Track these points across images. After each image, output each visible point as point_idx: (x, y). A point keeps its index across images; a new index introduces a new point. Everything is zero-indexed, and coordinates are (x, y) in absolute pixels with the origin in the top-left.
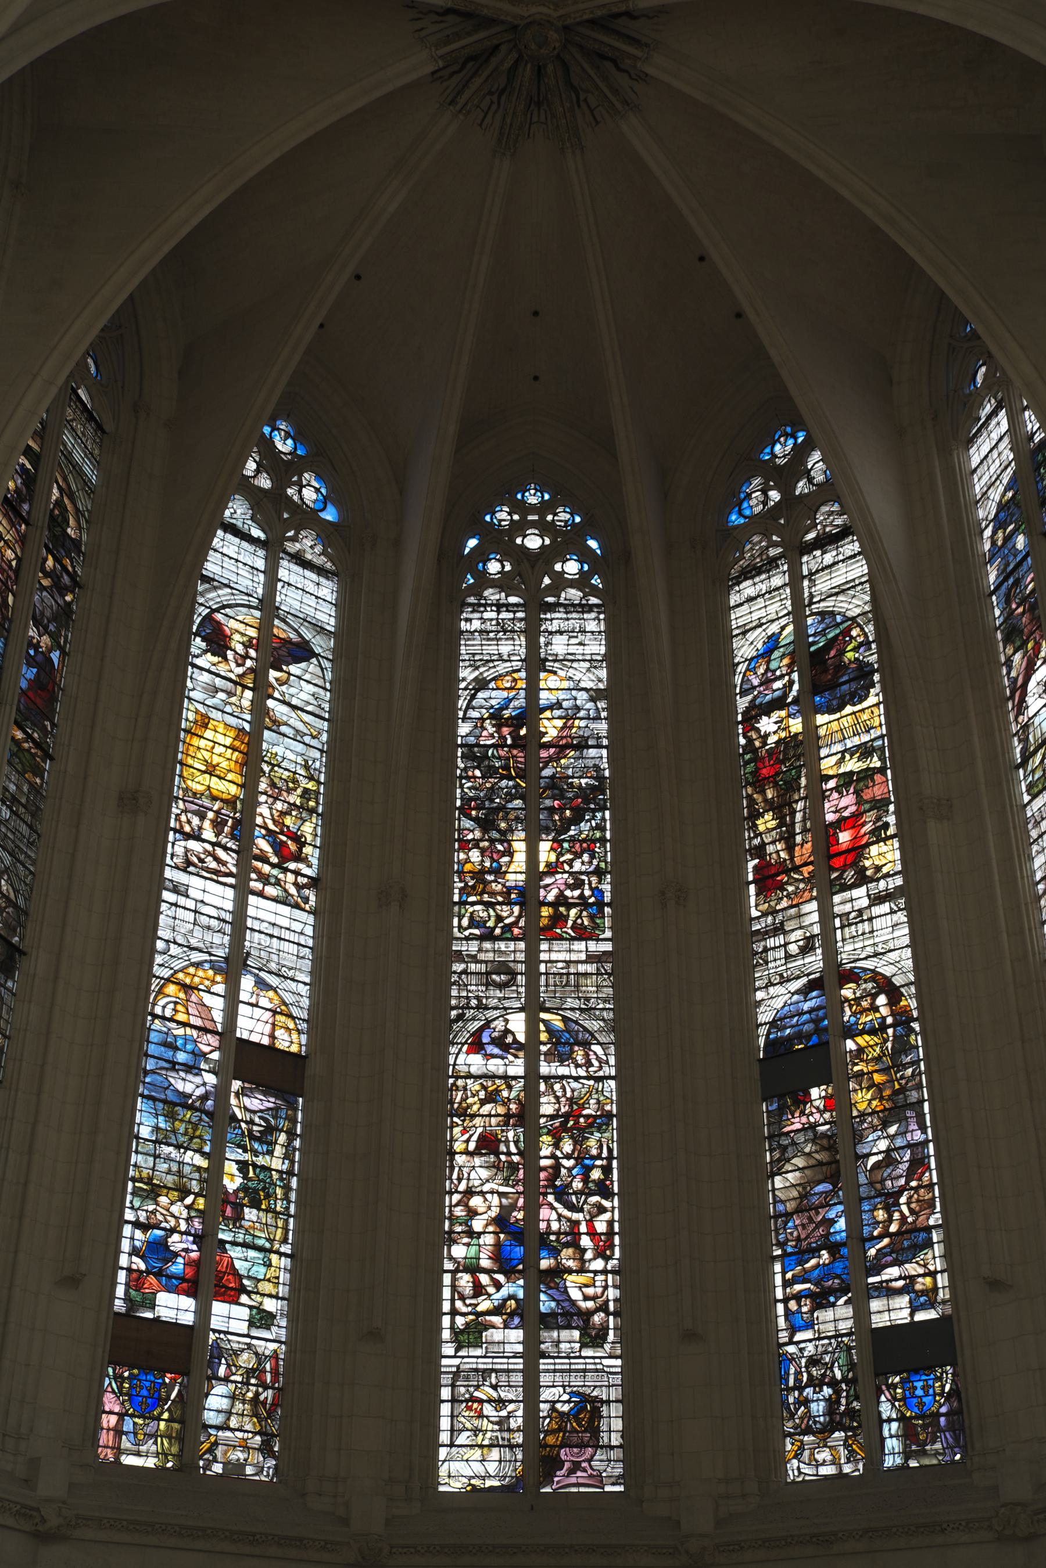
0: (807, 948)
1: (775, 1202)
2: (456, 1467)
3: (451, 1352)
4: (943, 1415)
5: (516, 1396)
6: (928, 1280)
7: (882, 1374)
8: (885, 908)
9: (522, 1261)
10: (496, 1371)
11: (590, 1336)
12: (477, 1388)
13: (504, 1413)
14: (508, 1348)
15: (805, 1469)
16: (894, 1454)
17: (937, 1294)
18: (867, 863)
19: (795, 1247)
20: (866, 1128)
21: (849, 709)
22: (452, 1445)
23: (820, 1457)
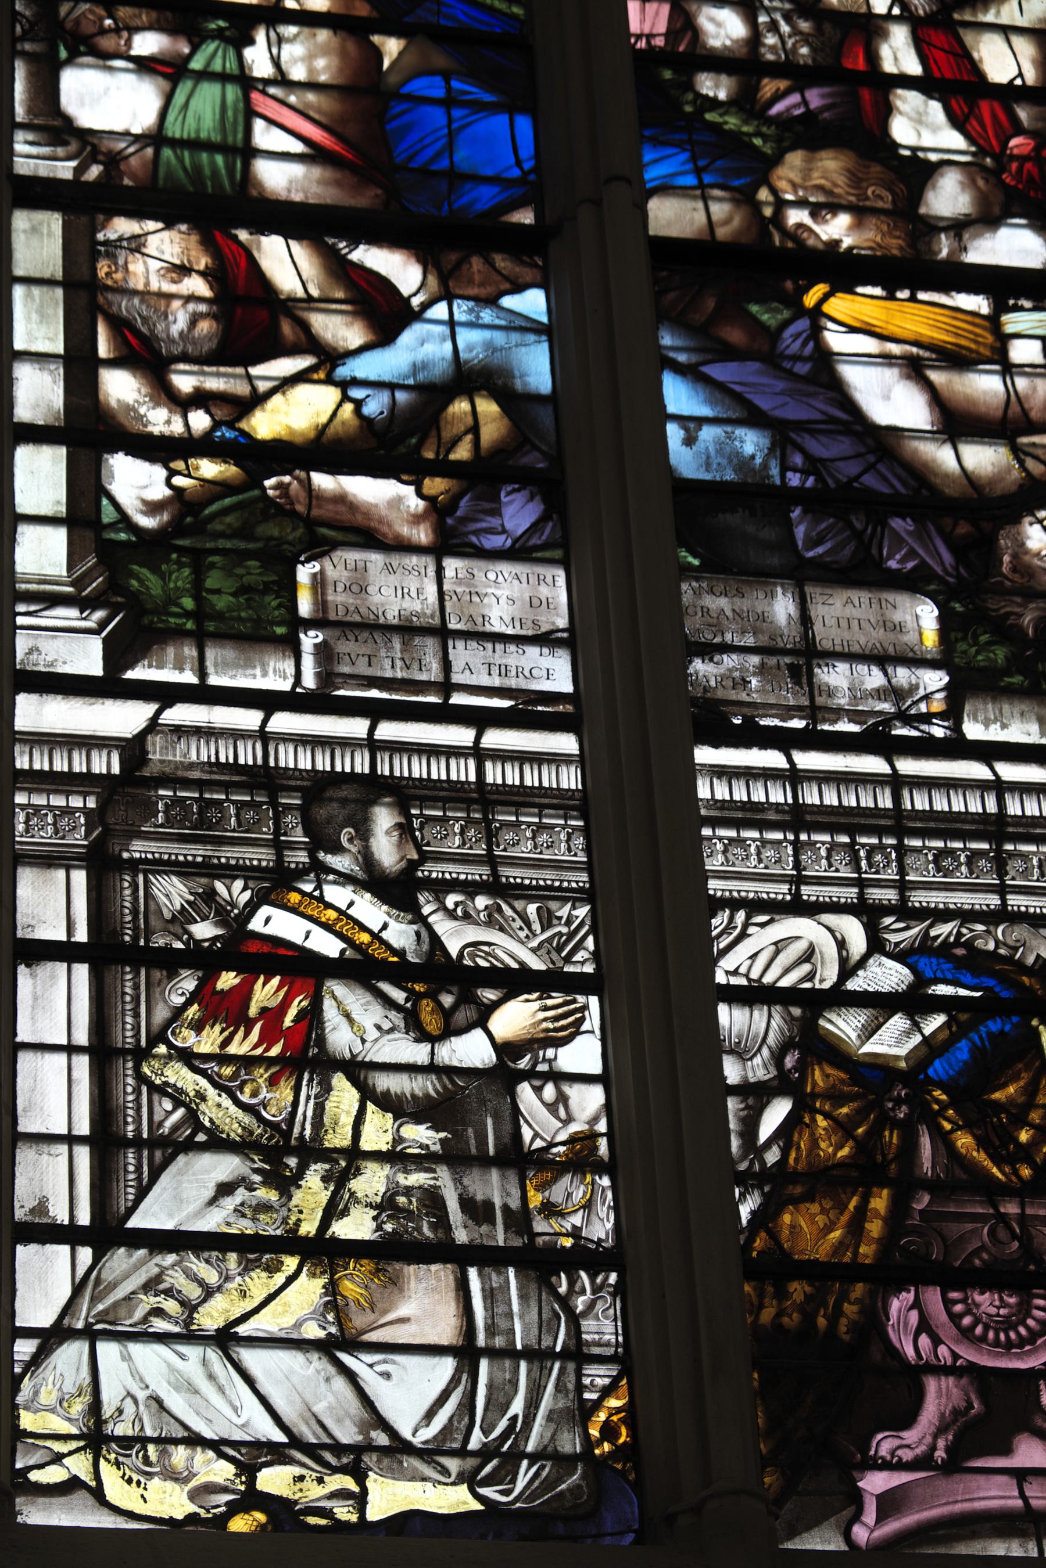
2: (136, 1374)
3: (87, 658)
5: (552, 947)
9: (527, 189)
10: (404, 794)
11: (1005, 631)
12: (275, 885)
13: (472, 1050)
14: (470, 663)
22: (107, 1232)
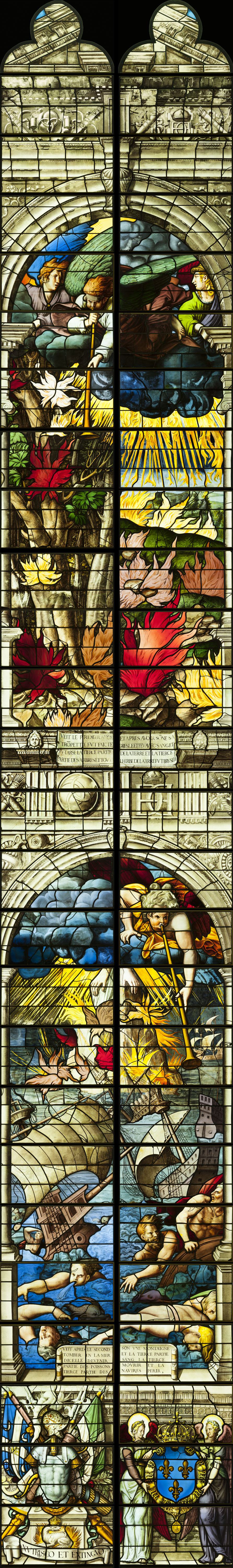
0: (89, 808)
8: (200, 779)
18: (181, 697)
21: (175, 419)
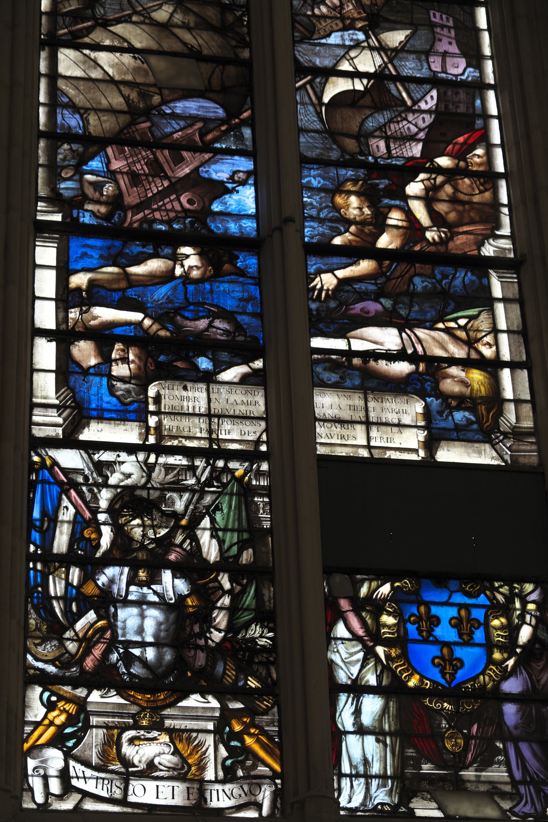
1: (53, 105)
4: (510, 698)
6: (477, 376)
7: (342, 571)
15: (87, 781)
16: (368, 777)
17: (500, 413)
19: (108, 217)
20: (324, 17)
23: (139, 754)
